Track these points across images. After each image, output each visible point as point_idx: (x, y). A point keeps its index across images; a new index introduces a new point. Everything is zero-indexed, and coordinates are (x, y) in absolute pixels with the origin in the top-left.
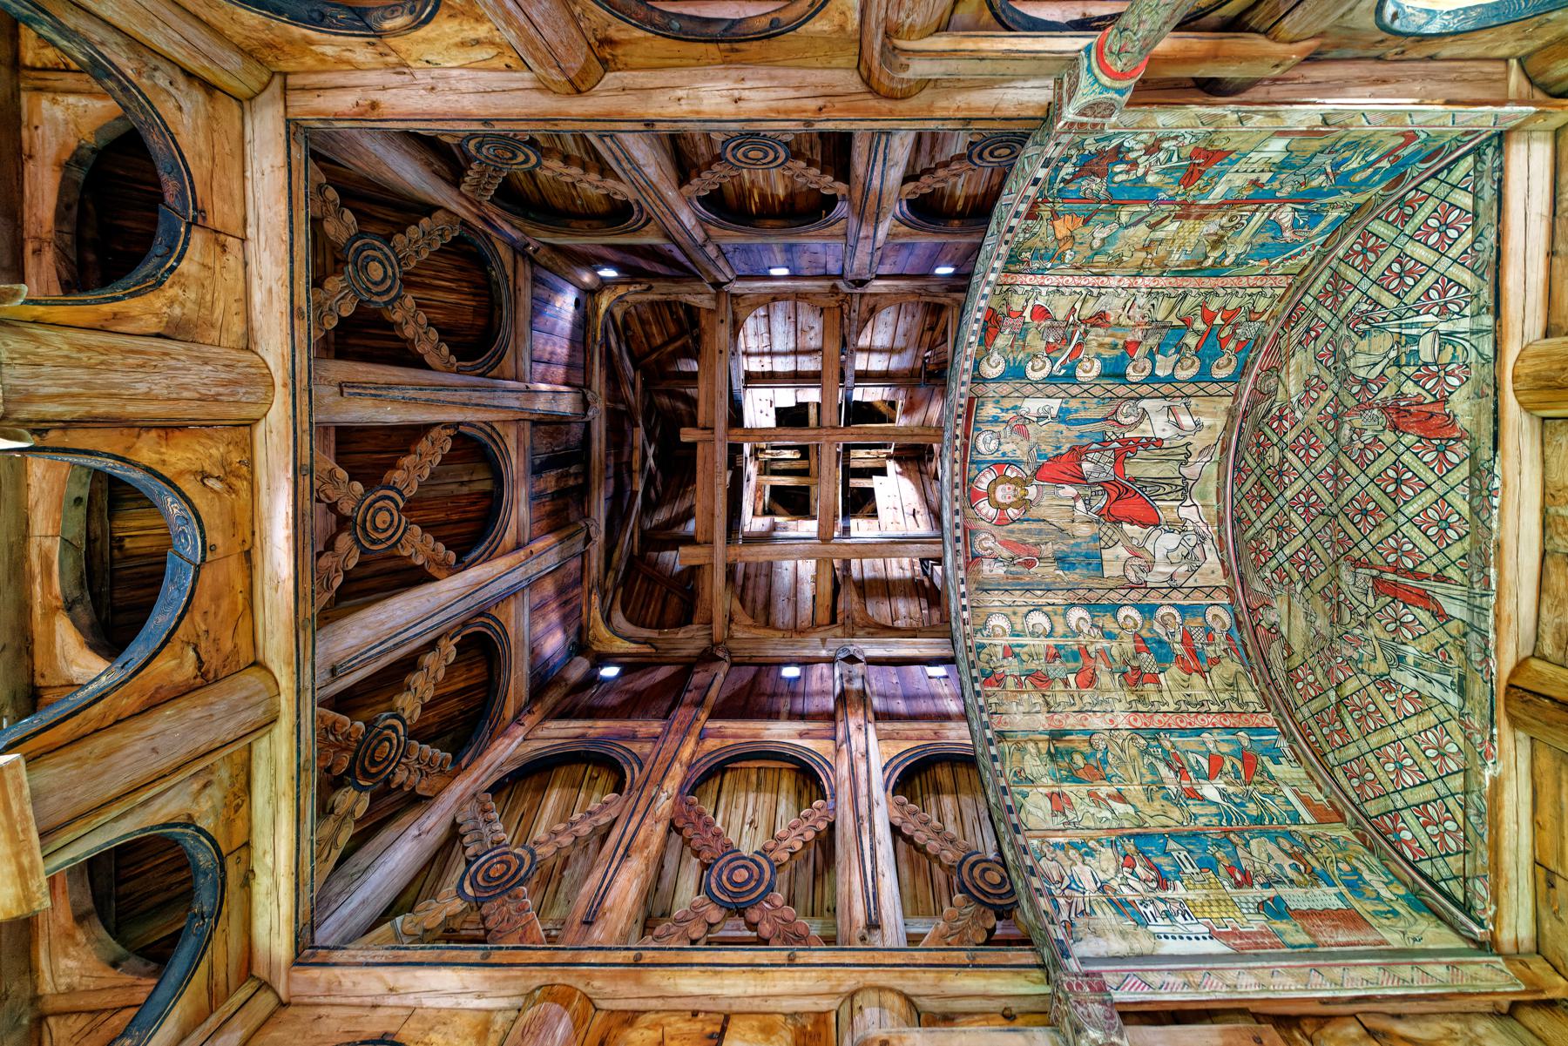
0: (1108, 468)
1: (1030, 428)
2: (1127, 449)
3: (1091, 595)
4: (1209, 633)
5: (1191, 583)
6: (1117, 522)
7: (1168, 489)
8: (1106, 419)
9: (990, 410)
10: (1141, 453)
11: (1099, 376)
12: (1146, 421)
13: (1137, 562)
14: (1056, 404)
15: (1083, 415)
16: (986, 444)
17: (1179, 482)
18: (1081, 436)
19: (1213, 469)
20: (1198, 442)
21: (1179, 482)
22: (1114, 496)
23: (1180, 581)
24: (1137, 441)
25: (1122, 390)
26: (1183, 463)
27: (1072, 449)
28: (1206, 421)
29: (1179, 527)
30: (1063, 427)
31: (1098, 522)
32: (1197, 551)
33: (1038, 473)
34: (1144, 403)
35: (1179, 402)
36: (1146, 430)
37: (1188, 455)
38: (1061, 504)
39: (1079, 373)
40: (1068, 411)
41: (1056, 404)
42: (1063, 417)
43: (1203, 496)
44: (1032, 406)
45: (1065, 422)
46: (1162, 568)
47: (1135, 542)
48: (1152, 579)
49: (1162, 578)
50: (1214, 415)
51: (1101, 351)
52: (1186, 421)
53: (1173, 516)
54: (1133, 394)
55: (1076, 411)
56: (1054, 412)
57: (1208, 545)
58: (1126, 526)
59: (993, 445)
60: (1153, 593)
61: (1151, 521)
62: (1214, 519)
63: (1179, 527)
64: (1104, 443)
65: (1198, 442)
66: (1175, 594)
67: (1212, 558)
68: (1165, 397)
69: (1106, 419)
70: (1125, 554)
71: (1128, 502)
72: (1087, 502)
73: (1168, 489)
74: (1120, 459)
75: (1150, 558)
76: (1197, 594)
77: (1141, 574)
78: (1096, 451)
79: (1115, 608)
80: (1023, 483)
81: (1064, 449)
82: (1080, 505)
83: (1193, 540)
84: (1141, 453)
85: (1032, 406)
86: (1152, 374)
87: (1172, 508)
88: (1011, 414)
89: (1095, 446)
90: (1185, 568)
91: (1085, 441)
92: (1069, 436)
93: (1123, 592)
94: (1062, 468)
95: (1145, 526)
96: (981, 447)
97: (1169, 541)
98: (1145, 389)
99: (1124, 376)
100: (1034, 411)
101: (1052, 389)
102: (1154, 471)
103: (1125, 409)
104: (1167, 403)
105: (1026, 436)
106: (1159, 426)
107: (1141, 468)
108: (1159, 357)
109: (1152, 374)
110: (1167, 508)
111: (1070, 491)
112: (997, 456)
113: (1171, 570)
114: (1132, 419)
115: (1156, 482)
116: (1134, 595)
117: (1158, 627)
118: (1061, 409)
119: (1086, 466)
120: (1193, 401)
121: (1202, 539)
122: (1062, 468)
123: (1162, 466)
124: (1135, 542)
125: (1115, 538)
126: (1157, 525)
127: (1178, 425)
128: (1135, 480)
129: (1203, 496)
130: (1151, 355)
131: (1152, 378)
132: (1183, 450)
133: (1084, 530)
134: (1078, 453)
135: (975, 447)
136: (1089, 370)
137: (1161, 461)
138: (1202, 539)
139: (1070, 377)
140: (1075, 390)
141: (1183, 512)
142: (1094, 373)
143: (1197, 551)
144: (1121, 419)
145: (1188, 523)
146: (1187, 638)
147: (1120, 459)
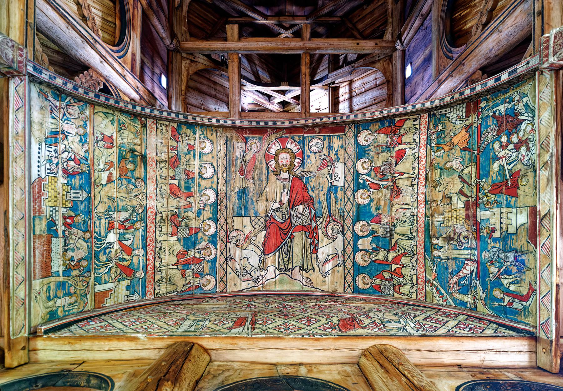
0: (299, 221)
1: (325, 171)
2: (311, 233)
3: (223, 208)
4: (200, 275)
5: (229, 270)
6: (266, 227)
7: (286, 259)
8: (330, 215)
9: (336, 143)
10: (309, 241)
11: (358, 205)
12: (329, 241)
13: (242, 238)
14: (340, 183)
15: (333, 201)
16: (315, 144)
17: (290, 266)
18: (319, 203)
19: (297, 286)
20: (315, 276)
21: (290, 266)
22: (282, 226)
23: (230, 263)
24: (316, 238)
25: (349, 222)
26: (302, 268)
27: (311, 198)
28: (328, 279)
29: (262, 267)
30: (326, 190)
31: (266, 216)
32: (248, 277)
33: (297, 178)
34: (340, 237)
35: (341, 259)
36: (323, 241)
37: (307, 271)
38: (277, 192)
39: (360, 192)
40: (336, 191)
41: (340, 183)
42: (332, 189)
43: (281, 282)
44: (339, 170)
45: (329, 190)
46: (238, 254)
47: (254, 238)
48: (231, 246)
49: (232, 253)
50: (332, 283)
51: (375, 201)
52: (329, 266)
53: (269, 263)
54: (346, 229)
55: (335, 197)
56: (335, 183)
57: (252, 284)
58: (263, 233)
59: (314, 149)
60: (223, 246)
61: (266, 249)
62: (267, 288)
63: (262, 267)
64: (315, 217)
65: (315, 276)
66: (223, 260)
67: (244, 286)
68: (344, 250)
69: (330, 215)
70: (247, 231)
71: (279, 235)
72: (278, 210)
73: (286, 259)
74: (304, 228)
75: (244, 247)
76: (223, 273)
77: (234, 240)
78: (310, 213)
79: (215, 219)
80: (291, 170)
81: (311, 193)
82: (277, 205)
83: (255, 275)
84: (309, 241)
85: (339, 170)
86: (359, 237)
87: (275, 262)
88: (333, 156)
89: (313, 212)
90: (238, 268)
91: (317, 206)
92: (319, 195)
93: (224, 227)
94: (300, 192)
95: (264, 245)
96: (313, 142)
97: (254, 260)
98: (349, 235)
99: (358, 220)
100: (336, 170)
101: (350, 178)
102: (297, 250)
103: (337, 227)
104: (340, 253)
105: (320, 169)
106: (326, 249)
107: (299, 241)
108: (370, 238)
109: (359, 237)
110: (273, 259)
111: (286, 199)
112: (307, 152)
113: (237, 258)
114: (330, 232)
115: (290, 252)
116: (223, 234)
117: (203, 244)
118: (337, 187)
119: (301, 208)
120: (341, 268)
121: (255, 280)
122: (300, 192)
123: (300, 255)
124: (254, 238)
125: (257, 226)
126: (264, 252)
127: (326, 261)
128: (292, 239)
129: (281, 282)
130: (372, 233)
131: (356, 238)
132: (310, 267)
133: (261, 207)
134: (309, 202)
135: (313, 138)
136: (362, 198)
137: (303, 255)
138: (255, 280)
139: (358, 187)
140: (349, 192)
141: (271, 269)
142: (361, 201)
143: (248, 277)
144: (330, 225)
145: (265, 272)
146: (199, 261)
147: (304, 228)
